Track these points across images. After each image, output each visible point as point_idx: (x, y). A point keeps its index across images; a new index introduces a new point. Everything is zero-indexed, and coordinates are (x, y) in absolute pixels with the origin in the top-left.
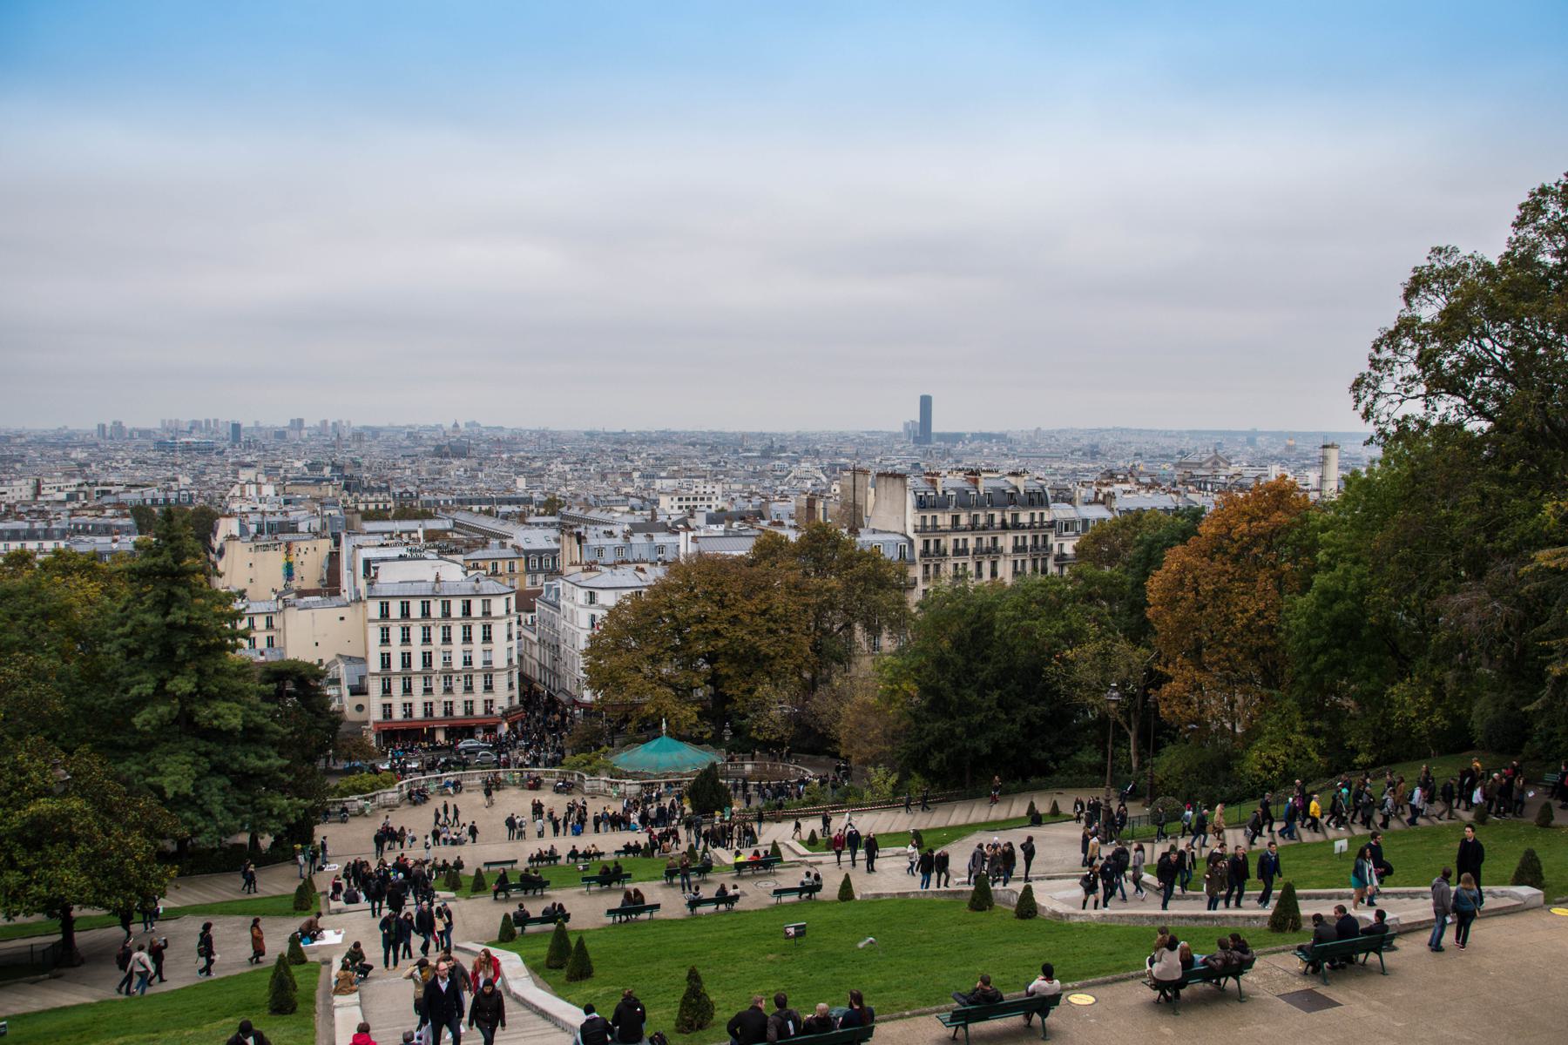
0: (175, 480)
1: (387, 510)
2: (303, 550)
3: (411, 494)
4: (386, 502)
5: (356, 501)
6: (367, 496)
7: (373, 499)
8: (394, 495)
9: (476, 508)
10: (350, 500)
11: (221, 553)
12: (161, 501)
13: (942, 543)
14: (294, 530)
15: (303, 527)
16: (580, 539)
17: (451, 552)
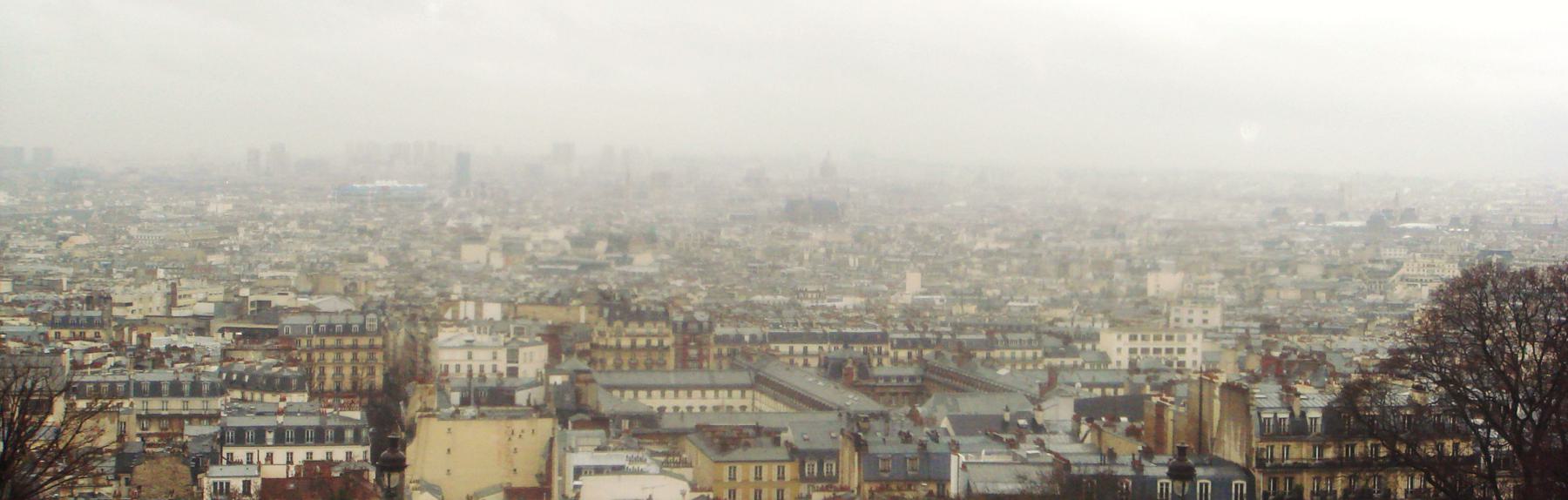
0: (363, 260)
1: (663, 349)
2: (518, 433)
3: (700, 324)
4: (661, 336)
5: (618, 334)
6: (634, 327)
7: (642, 331)
8: (675, 325)
9: (798, 348)
10: (608, 331)
11: (411, 432)
12: (339, 328)
13: (1297, 481)
14: (510, 400)
15: (521, 397)
16: (860, 445)
17: (677, 465)
